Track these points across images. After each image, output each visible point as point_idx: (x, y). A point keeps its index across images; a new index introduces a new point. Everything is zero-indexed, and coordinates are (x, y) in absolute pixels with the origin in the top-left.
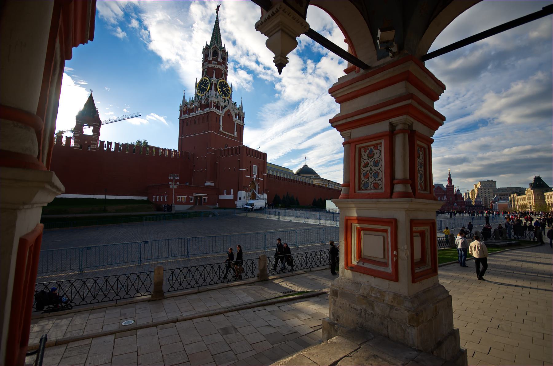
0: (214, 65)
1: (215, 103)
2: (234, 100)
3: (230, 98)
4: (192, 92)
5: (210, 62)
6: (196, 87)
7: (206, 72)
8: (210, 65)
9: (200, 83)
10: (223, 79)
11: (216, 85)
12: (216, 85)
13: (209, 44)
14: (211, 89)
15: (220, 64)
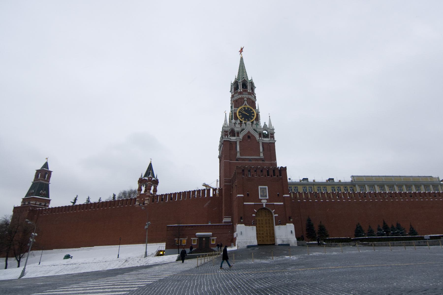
5: (250, 94)
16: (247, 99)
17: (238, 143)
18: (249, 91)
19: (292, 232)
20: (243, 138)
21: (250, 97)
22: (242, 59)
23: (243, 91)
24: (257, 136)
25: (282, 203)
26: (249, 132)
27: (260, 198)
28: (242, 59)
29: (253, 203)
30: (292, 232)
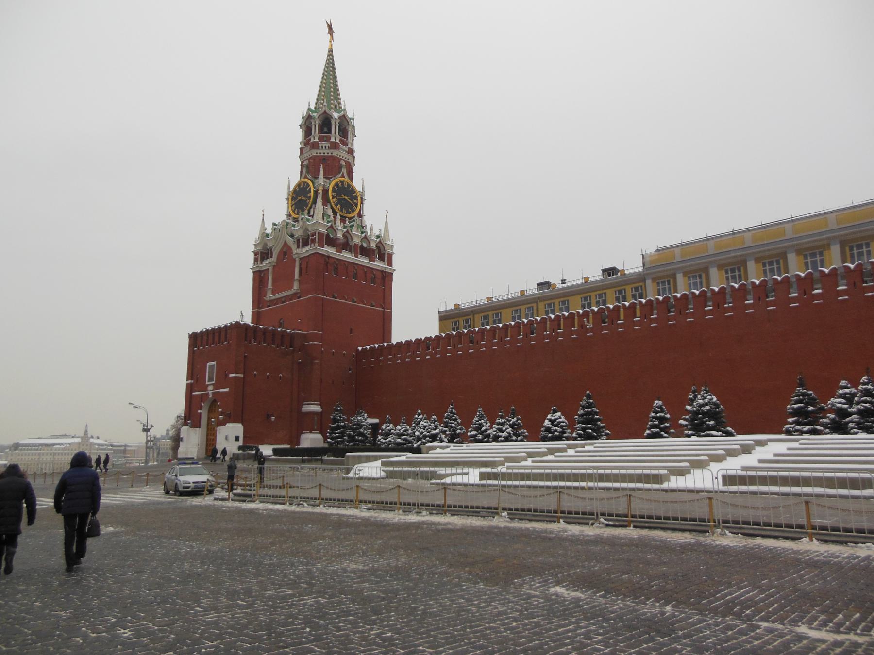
0: (324, 151)
1: (320, 235)
2: (368, 220)
3: (360, 215)
4: (278, 211)
5: (315, 146)
6: (288, 199)
7: (308, 167)
8: (314, 153)
9: (295, 190)
10: (343, 176)
11: (325, 192)
12: (325, 192)
13: (313, 107)
14: (315, 202)
15: (335, 146)
16: (309, 159)
17: (270, 271)
18: (312, 140)
19: (227, 438)
20: (278, 259)
21: (314, 153)
22: (331, 51)
23: (327, 134)
24: (294, 247)
25: (227, 390)
26: (285, 244)
27: (207, 383)
28: (331, 51)
29: (200, 393)
30: (227, 438)
